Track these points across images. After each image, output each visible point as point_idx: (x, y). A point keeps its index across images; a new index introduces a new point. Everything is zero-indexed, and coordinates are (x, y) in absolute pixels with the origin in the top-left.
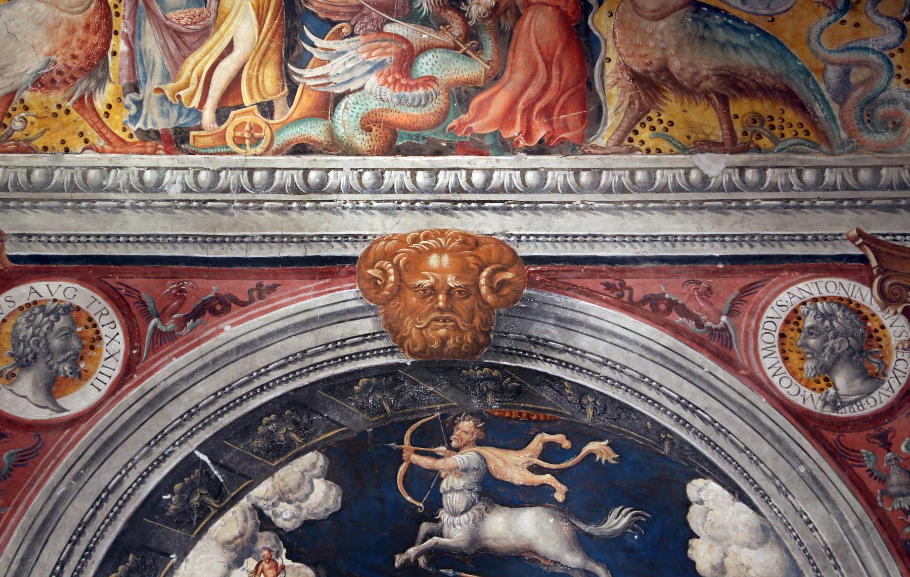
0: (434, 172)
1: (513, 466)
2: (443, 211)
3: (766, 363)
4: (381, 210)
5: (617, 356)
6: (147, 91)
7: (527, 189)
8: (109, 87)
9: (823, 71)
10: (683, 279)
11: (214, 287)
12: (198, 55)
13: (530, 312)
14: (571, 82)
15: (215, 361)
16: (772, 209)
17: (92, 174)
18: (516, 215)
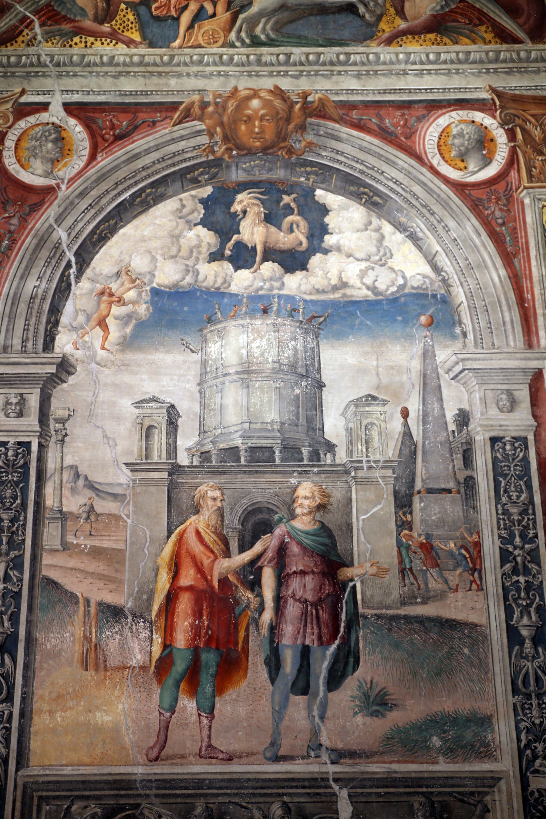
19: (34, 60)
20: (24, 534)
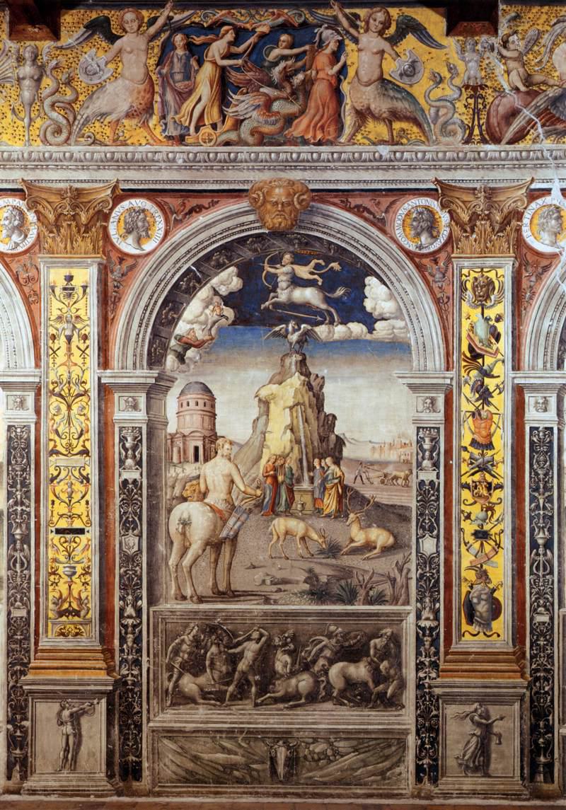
0: (278, 153)
1: (303, 272)
2: (281, 170)
3: (397, 232)
4: (258, 169)
5: (343, 229)
6: (169, 118)
7: (314, 161)
8: (154, 117)
9: (429, 110)
10: (370, 198)
11: (193, 202)
12: (188, 102)
13: (312, 212)
14: (333, 113)
15: (197, 231)
16: (405, 169)
17: (150, 155)
18: (309, 172)
19: (539, 155)
20: (552, 482)
